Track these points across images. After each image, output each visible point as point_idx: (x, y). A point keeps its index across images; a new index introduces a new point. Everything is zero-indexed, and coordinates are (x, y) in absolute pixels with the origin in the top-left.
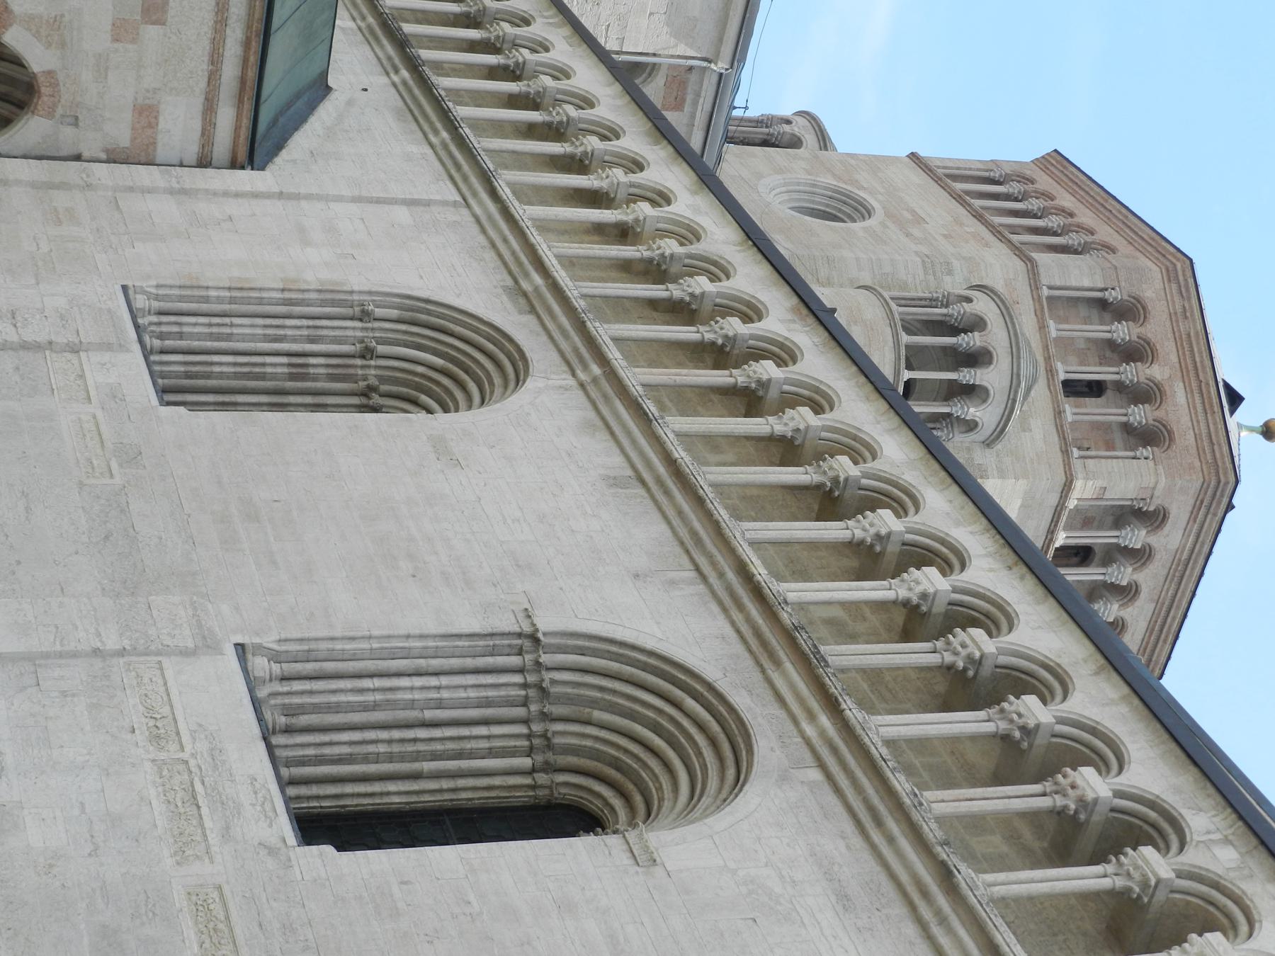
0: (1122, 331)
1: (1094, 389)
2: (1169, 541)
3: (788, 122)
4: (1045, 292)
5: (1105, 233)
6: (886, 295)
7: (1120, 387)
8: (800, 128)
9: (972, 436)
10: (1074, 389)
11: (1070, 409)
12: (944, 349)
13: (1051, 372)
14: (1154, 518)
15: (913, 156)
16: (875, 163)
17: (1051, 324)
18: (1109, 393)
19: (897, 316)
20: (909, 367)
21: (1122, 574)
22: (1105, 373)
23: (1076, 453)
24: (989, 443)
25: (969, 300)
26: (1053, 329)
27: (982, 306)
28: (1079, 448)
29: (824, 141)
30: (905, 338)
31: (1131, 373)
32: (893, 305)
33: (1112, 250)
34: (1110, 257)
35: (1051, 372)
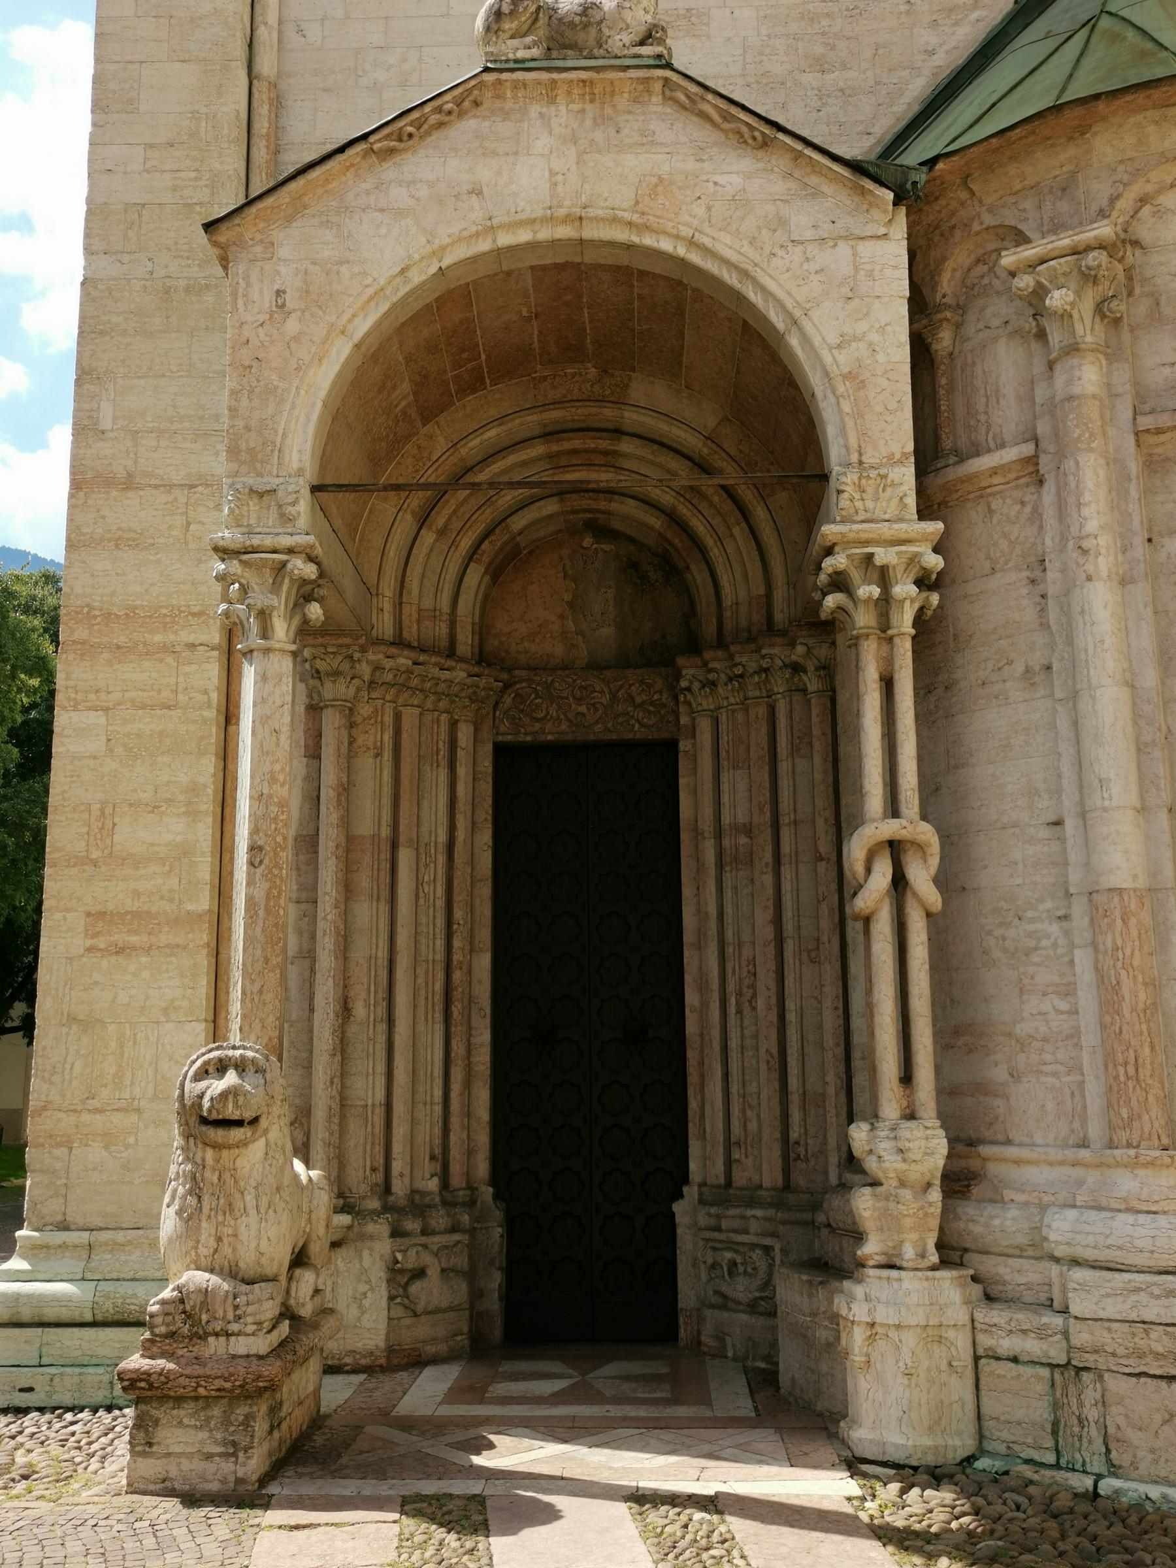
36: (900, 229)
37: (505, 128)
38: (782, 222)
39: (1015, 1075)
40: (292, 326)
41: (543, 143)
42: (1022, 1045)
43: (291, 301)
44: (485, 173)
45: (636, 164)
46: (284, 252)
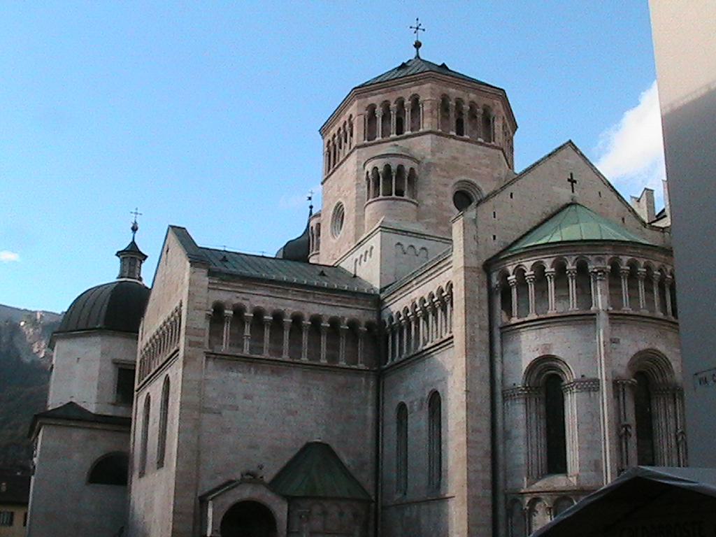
0: (379, 111)
2: (453, 92)
4: (366, 142)
5: (344, 118)
6: (367, 203)
7: (398, 113)
9: (416, 170)
10: (400, 130)
11: (408, 133)
12: (384, 179)
14: (445, 98)
15: (322, 184)
17: (377, 139)
19: (373, 200)
20: (391, 195)
21: (466, 107)
22: (394, 118)
23: (421, 130)
25: (368, 173)
26: (379, 139)
27: (369, 167)
28: (420, 128)
30: (381, 197)
32: (370, 200)
33: (351, 116)
34: (354, 116)
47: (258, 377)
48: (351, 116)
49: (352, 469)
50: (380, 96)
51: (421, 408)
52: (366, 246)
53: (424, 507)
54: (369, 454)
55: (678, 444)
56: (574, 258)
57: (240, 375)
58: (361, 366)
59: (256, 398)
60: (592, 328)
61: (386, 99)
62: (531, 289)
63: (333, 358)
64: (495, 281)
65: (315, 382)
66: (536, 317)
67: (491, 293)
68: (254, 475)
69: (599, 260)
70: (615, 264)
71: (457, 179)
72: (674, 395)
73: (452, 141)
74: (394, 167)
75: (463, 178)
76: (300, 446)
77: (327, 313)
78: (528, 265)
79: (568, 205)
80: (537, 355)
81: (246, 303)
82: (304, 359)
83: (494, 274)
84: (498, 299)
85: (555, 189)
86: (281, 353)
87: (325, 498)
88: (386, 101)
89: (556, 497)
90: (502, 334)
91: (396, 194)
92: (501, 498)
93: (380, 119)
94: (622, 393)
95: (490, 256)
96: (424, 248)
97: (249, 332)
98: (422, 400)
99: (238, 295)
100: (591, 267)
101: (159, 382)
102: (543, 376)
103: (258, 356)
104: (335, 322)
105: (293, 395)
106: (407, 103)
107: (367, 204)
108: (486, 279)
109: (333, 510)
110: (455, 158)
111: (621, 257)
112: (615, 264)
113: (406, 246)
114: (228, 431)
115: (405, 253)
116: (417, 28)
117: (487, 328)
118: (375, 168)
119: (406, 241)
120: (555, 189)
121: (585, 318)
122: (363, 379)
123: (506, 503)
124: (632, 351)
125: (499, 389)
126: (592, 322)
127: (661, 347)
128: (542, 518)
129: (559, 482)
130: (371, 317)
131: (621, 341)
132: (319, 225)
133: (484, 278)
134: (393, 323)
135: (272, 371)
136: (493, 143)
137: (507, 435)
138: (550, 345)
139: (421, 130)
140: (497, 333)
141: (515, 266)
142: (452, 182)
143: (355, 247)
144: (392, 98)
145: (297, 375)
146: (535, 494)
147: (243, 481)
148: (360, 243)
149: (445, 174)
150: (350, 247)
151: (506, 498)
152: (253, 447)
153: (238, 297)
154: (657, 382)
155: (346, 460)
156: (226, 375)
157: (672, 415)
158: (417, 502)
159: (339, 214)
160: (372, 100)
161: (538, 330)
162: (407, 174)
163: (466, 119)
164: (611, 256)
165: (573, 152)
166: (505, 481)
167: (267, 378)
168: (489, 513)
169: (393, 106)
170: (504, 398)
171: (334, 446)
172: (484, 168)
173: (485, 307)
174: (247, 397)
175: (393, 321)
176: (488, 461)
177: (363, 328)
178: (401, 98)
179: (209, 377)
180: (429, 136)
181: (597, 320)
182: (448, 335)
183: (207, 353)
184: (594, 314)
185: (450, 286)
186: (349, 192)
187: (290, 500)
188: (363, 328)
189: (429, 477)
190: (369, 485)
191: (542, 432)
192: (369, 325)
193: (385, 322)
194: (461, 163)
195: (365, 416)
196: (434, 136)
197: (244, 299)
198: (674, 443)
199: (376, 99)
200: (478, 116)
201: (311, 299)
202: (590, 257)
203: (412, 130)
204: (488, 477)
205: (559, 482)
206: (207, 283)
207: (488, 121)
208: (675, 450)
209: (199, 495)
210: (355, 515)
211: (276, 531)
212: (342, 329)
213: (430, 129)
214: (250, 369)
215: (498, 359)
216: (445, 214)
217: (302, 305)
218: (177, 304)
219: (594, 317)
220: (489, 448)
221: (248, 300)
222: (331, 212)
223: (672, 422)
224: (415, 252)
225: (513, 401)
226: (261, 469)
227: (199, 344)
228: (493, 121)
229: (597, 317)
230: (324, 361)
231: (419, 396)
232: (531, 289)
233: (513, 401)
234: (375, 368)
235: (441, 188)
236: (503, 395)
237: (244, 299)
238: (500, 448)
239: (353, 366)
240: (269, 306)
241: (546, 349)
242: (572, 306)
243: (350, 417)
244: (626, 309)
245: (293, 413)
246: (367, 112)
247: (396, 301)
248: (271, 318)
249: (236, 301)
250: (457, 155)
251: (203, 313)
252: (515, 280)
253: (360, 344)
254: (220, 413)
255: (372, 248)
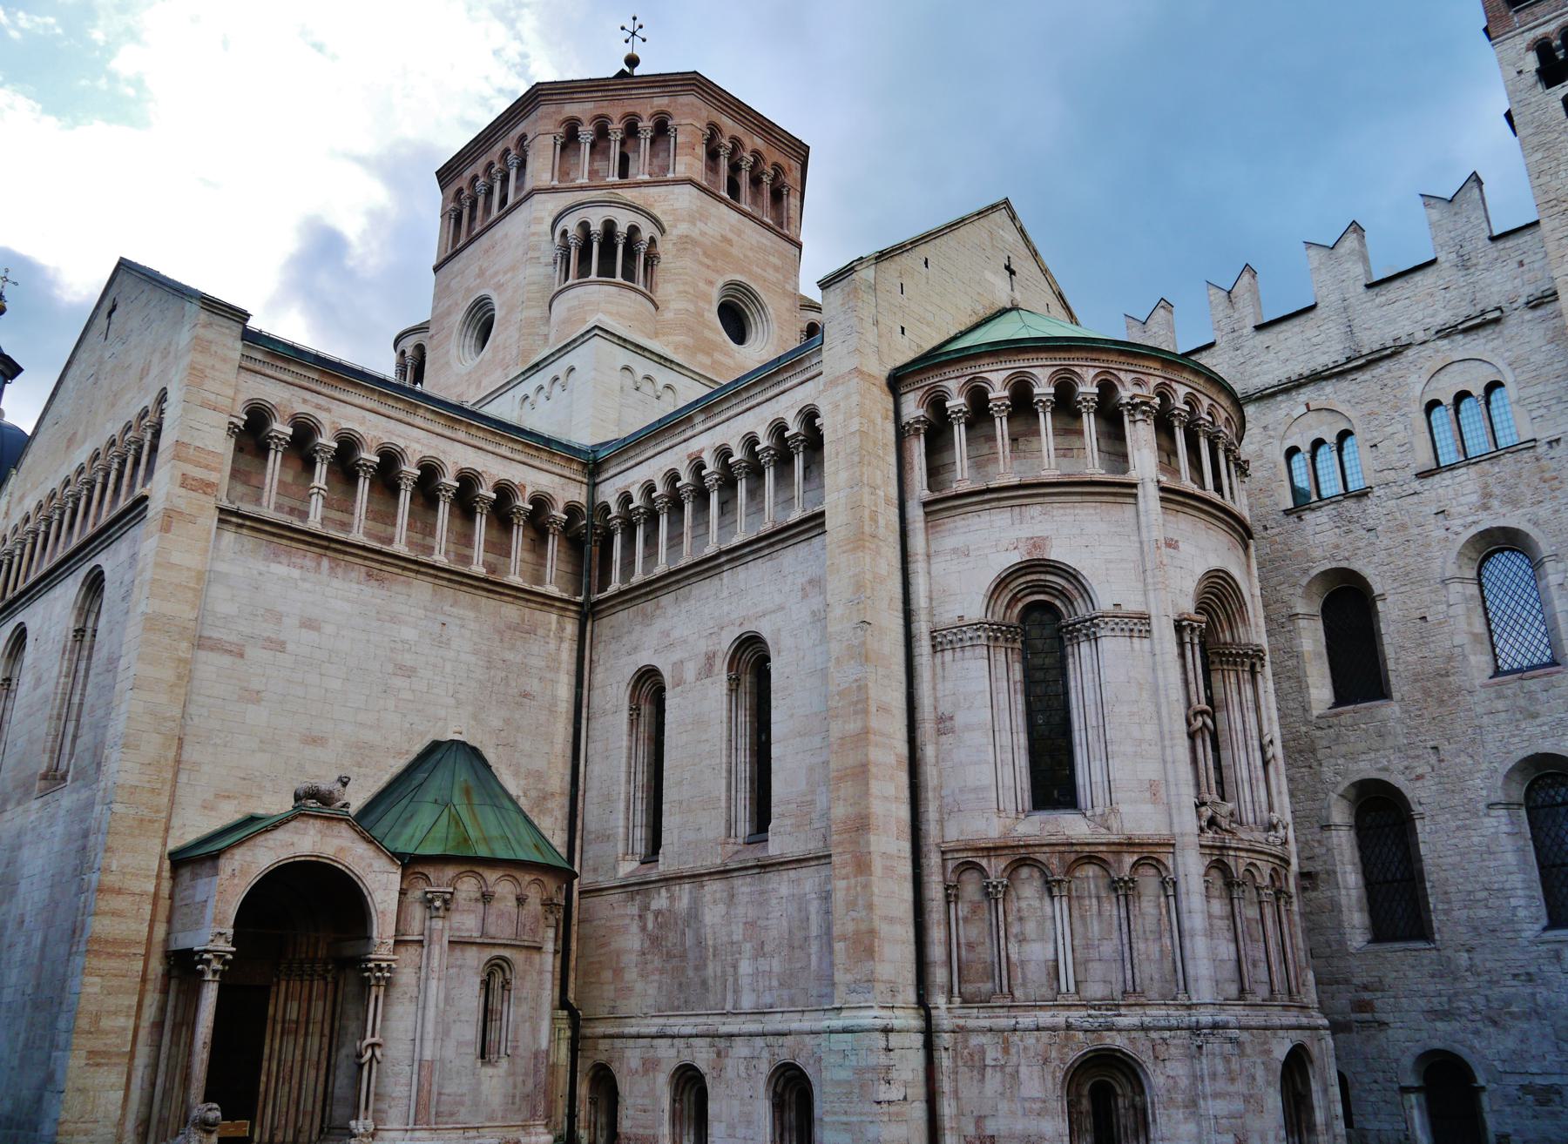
0: (586, 133)
1: (624, 161)
3: (403, 353)
5: (510, 141)
8: (409, 345)
10: (623, 173)
13: (614, 186)
15: (436, 269)
16: (441, 292)
18: (625, 150)
22: (615, 151)
24: (663, 231)
25: (564, 233)
27: (571, 224)
29: (422, 328)
31: (616, 134)
32: (568, 283)
35: (614, 186)
36: (399, 871)
37: (302, 826)
38: (371, 865)
39: (390, 1107)
40: (236, 881)
41: (312, 832)
42: (393, 1099)
43: (236, 872)
44: (295, 839)
45: (337, 842)
46: (237, 857)
47: (336, 583)
48: (523, 137)
49: (524, 803)
50: (589, 106)
51: (708, 669)
52: (559, 368)
53: (714, 888)
54: (558, 780)
55: (1266, 763)
56: (1092, 372)
57: (296, 573)
58: (552, 589)
59: (329, 629)
60: (1129, 511)
61: (599, 112)
62: (1002, 427)
63: (491, 568)
64: (913, 408)
65: (454, 610)
66: (1015, 481)
67: (902, 434)
68: (324, 798)
69: (1138, 383)
70: (1164, 393)
71: (729, 277)
72: (1253, 666)
73: (723, 207)
74: (622, 228)
75: (738, 277)
76: (418, 748)
77: (494, 472)
78: (997, 382)
79: (1003, 312)
80: (1015, 558)
81: (322, 416)
82: (439, 559)
83: (911, 396)
84: (918, 449)
85: (989, 275)
86: (390, 541)
87: (492, 863)
88: (600, 116)
89: (1073, 857)
90: (927, 514)
91: (623, 276)
92: (933, 860)
93: (588, 145)
94: (1189, 646)
95: (898, 364)
96: (668, 387)
97: (323, 481)
98: (710, 658)
99: (308, 395)
100: (1125, 394)
101: (69, 590)
102: (1020, 605)
103: (342, 536)
104: (505, 491)
105: (409, 633)
106: (646, 125)
107: (560, 292)
108: (891, 406)
109: (504, 889)
110: (725, 239)
111: (1174, 385)
112: (1164, 393)
113: (640, 372)
114: (256, 697)
115: (637, 389)
116: (634, 34)
117: (896, 502)
118: (584, 226)
119: (642, 366)
120: (989, 275)
121: (1126, 491)
122: (554, 617)
123: (944, 874)
124: (1200, 570)
125: (922, 628)
126: (1131, 500)
127: (1236, 572)
128: (1037, 904)
129: (1072, 826)
130: (578, 494)
131: (1180, 544)
132: (420, 349)
133: (889, 401)
134: (631, 506)
135: (369, 575)
136: (786, 232)
137: (944, 723)
138: (1044, 539)
139: (670, 176)
140: (916, 513)
141: (963, 380)
142: (720, 283)
143: (523, 373)
144: (615, 114)
145: (422, 589)
146: (1022, 851)
147: (298, 814)
148: (537, 365)
149: (706, 261)
150: (506, 376)
151: (944, 860)
152: (315, 740)
153: (305, 401)
154: (1222, 640)
155: (512, 785)
156: (263, 569)
157: (1251, 705)
158: (696, 877)
159: (482, 322)
160: (572, 110)
161: (1017, 509)
162: (643, 248)
163: (744, 179)
164: (1160, 380)
165: (1008, 221)
166: (941, 822)
167: (355, 586)
168: (908, 893)
169: (616, 128)
170: (934, 646)
171: (490, 755)
172: (770, 271)
173: (892, 459)
174: (309, 624)
175: (631, 501)
176: (903, 778)
177: (558, 513)
178: (634, 114)
179: (222, 567)
180: (688, 188)
181: (1140, 499)
182: (795, 515)
183: (221, 510)
184: (1134, 486)
185: (810, 416)
186: (509, 275)
187: (410, 864)
188: (558, 513)
189: (729, 822)
190: (558, 840)
191: (1020, 721)
192: (571, 509)
193: (607, 509)
194: (734, 251)
195: (554, 697)
196: (695, 191)
197: (318, 407)
198: (1259, 763)
199: (582, 110)
200: (765, 178)
201: (461, 435)
202: (1122, 375)
203: (651, 175)
204: (904, 812)
205: (1072, 826)
206: (237, 356)
207: (777, 196)
208: (1261, 773)
209: (172, 845)
210: (548, 904)
211: (369, 938)
212: (519, 508)
213: (688, 175)
214: (319, 564)
215: (918, 567)
216: (708, 334)
217: (443, 443)
218: (149, 401)
219: (1134, 491)
220: (903, 749)
221: (328, 410)
222: (459, 316)
223: (1251, 718)
224: (656, 391)
225: (959, 654)
226: (345, 784)
227: (206, 487)
228: (788, 195)
229: (1140, 491)
230: (478, 569)
231: (703, 646)
232: (1002, 427)
233: (959, 654)
234: (579, 599)
235: (702, 285)
236: (934, 638)
237: (318, 407)
238: (929, 752)
239: (537, 588)
240: (373, 433)
241: (1034, 546)
242: (1093, 466)
243: (525, 695)
244: (1187, 483)
245: (409, 672)
246: (561, 130)
247: (641, 462)
248: (377, 460)
249: (300, 408)
250: (730, 235)
251: (223, 421)
252: (965, 409)
253: (553, 545)
254: (241, 656)
255: (572, 369)
